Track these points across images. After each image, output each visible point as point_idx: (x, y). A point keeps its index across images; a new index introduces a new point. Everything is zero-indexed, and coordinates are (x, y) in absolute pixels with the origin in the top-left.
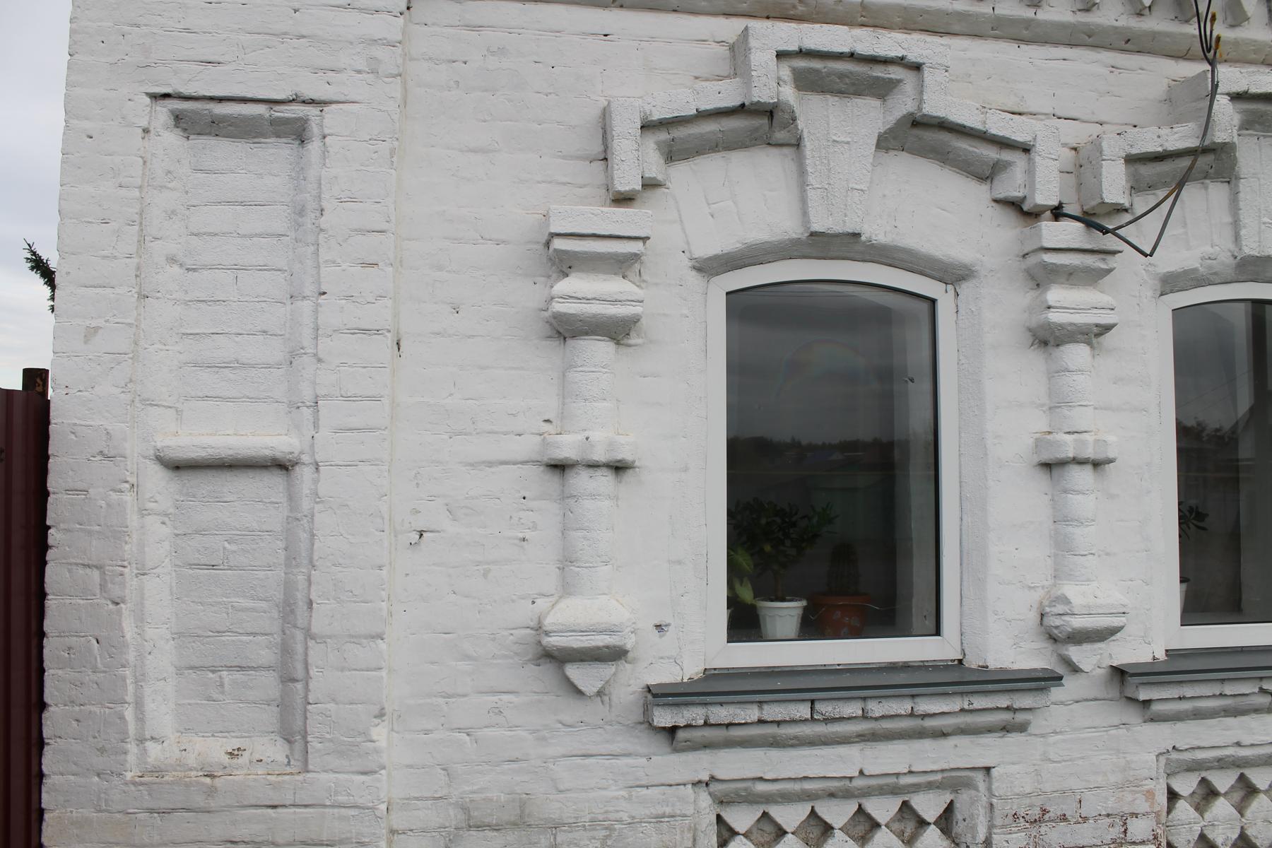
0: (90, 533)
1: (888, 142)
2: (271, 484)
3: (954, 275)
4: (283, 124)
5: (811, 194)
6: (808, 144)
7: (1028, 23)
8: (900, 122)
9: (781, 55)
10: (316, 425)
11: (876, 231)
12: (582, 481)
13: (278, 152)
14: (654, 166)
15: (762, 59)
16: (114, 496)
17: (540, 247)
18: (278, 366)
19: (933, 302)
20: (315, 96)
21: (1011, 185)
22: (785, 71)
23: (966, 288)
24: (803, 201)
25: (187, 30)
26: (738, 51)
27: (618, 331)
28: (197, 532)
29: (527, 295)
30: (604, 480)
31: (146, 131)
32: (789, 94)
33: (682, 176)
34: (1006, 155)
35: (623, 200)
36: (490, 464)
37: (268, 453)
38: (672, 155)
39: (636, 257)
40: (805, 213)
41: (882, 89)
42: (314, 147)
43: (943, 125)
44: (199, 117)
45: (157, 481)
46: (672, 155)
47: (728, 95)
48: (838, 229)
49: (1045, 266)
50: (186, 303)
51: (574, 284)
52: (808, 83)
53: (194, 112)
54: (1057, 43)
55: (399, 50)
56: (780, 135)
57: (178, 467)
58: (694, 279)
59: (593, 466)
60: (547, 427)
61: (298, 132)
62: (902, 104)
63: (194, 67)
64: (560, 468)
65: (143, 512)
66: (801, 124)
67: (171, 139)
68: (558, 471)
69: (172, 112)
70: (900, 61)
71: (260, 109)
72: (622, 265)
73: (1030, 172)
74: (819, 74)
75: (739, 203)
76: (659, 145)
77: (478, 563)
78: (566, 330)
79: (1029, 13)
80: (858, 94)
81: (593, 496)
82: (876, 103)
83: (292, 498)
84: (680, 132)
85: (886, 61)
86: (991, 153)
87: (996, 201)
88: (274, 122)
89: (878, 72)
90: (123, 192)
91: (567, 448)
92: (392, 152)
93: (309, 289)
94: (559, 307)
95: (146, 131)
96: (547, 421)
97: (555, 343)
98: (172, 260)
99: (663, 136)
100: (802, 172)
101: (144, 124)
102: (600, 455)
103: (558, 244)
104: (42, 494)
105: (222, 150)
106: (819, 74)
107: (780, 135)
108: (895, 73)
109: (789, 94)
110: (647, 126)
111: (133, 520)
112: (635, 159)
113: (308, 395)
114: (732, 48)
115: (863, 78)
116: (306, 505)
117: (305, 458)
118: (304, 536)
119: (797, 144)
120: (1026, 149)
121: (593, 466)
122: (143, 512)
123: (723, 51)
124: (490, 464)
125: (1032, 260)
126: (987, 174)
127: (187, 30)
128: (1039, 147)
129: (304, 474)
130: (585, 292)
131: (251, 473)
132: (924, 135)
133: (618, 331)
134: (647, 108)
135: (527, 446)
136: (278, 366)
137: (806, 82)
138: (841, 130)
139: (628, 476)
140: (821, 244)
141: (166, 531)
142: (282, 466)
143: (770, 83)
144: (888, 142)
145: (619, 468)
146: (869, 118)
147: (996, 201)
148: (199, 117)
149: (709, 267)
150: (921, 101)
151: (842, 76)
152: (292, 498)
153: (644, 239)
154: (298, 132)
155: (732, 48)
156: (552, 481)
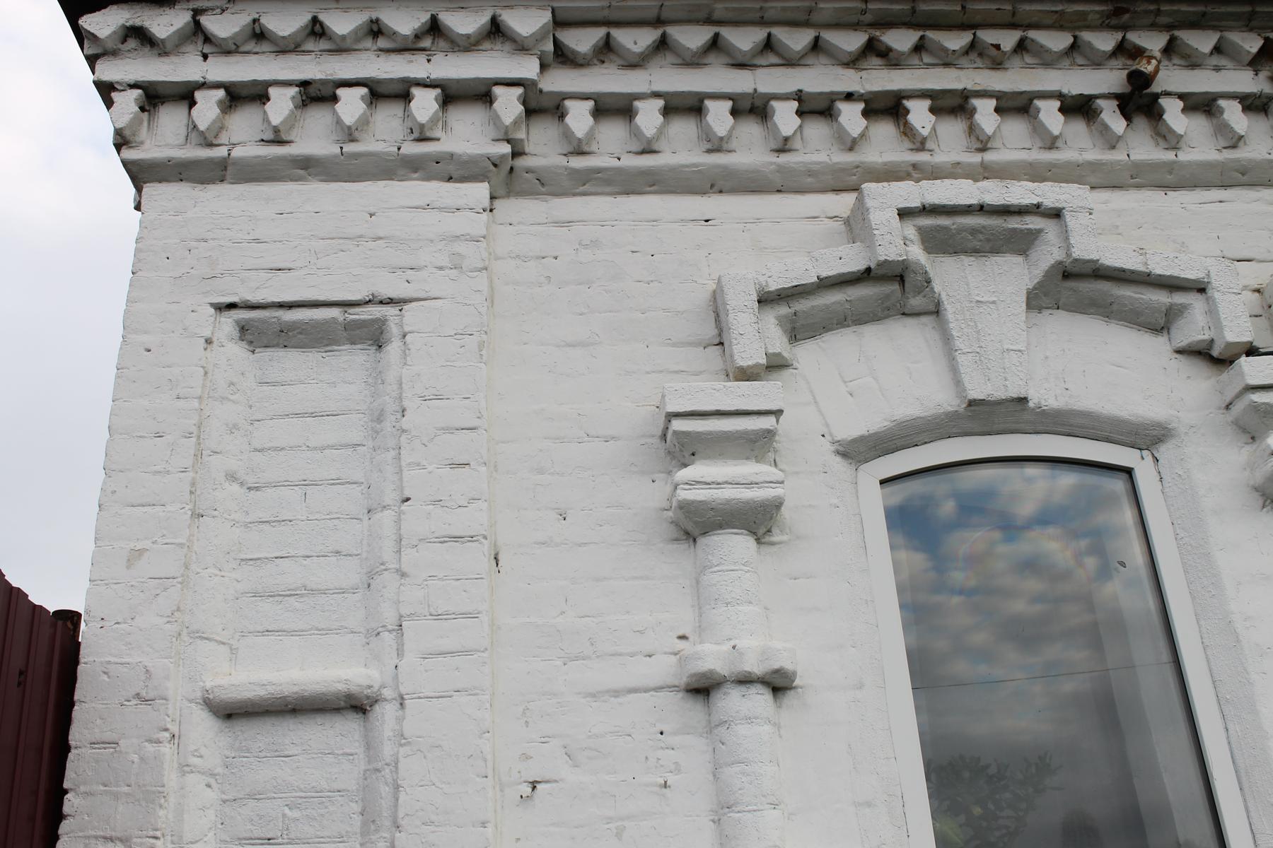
0: (116, 796)
1: (1038, 300)
2: (344, 731)
3: (1149, 437)
4: (360, 327)
5: (961, 359)
6: (949, 309)
7: (1170, 167)
8: (1049, 274)
9: (904, 214)
10: (400, 653)
11: (1045, 396)
12: (732, 701)
13: (351, 362)
14: (778, 342)
15: (882, 216)
16: (150, 748)
17: (656, 441)
18: (354, 590)
19: (1129, 472)
20: (393, 295)
21: (1194, 329)
22: (910, 230)
23: (1164, 451)
24: (954, 369)
25: (257, 241)
26: (856, 226)
27: (758, 521)
28: (252, 796)
29: (649, 496)
30: (760, 699)
31: (209, 341)
32: (916, 253)
33: (807, 355)
34: (1179, 298)
35: (746, 375)
36: (616, 693)
37: (341, 687)
38: (797, 332)
39: (769, 434)
40: (958, 383)
41: (1022, 244)
42: (393, 348)
43: (1099, 273)
44: (267, 326)
45: (203, 730)
46: (797, 332)
47: (852, 260)
48: (1001, 394)
49: (1255, 407)
50: (246, 525)
51: (697, 470)
52: (937, 243)
53: (259, 320)
54: (1208, 186)
55: (483, 244)
56: (916, 302)
57: (232, 713)
58: (838, 464)
59: (745, 681)
60: (682, 645)
61: (375, 336)
62: (1048, 254)
63: (263, 274)
64: (702, 689)
65: (185, 769)
66: (937, 286)
67: (237, 351)
68: (700, 697)
69: (237, 322)
70: (1036, 210)
71: (335, 313)
72: (758, 445)
73: (1212, 312)
74: (948, 230)
75: (879, 376)
76: (781, 321)
77: (610, 820)
78: (695, 524)
79: (1170, 156)
80: (996, 251)
81: (749, 720)
82: (1020, 259)
83: (370, 746)
84: (803, 305)
85: (1021, 211)
86: (1161, 298)
87: (1179, 351)
88: (350, 326)
89: (1014, 223)
90: (181, 403)
91: (711, 657)
92: (481, 346)
93: (391, 497)
94: (685, 494)
95: (209, 341)
96: (682, 637)
97: (683, 546)
98: (232, 477)
99: (784, 310)
100: (947, 338)
101: (207, 334)
102: (755, 667)
103: (677, 425)
104: (62, 749)
105: (289, 362)
106: (948, 230)
107: (916, 302)
108: (1033, 223)
109: (916, 253)
110: (766, 300)
111: (171, 779)
112: (756, 337)
113: (390, 617)
114: (847, 222)
115: (995, 232)
116: (388, 750)
117: (387, 693)
118: (385, 790)
119: (936, 311)
120: (1201, 288)
121: (745, 681)
122: (185, 769)
123: (839, 225)
124: (616, 693)
125: (1238, 407)
126: (1161, 324)
127: (257, 241)
128: (1215, 283)
129: (385, 714)
130: (718, 479)
131: (319, 719)
132: (1079, 286)
133: (758, 521)
134: (762, 279)
135: (664, 669)
136: (354, 590)
137: (937, 243)
138: (984, 293)
139: (789, 698)
140: (984, 415)
141: (212, 795)
142: (356, 705)
143: (896, 242)
144: (1038, 300)
145: (778, 685)
146: (1010, 278)
147: (1179, 351)
148: (267, 326)
149: (858, 451)
150: (1069, 247)
151: (974, 231)
152: (370, 746)
153: (778, 413)
154: (375, 336)
155: (847, 222)
156: (694, 710)
